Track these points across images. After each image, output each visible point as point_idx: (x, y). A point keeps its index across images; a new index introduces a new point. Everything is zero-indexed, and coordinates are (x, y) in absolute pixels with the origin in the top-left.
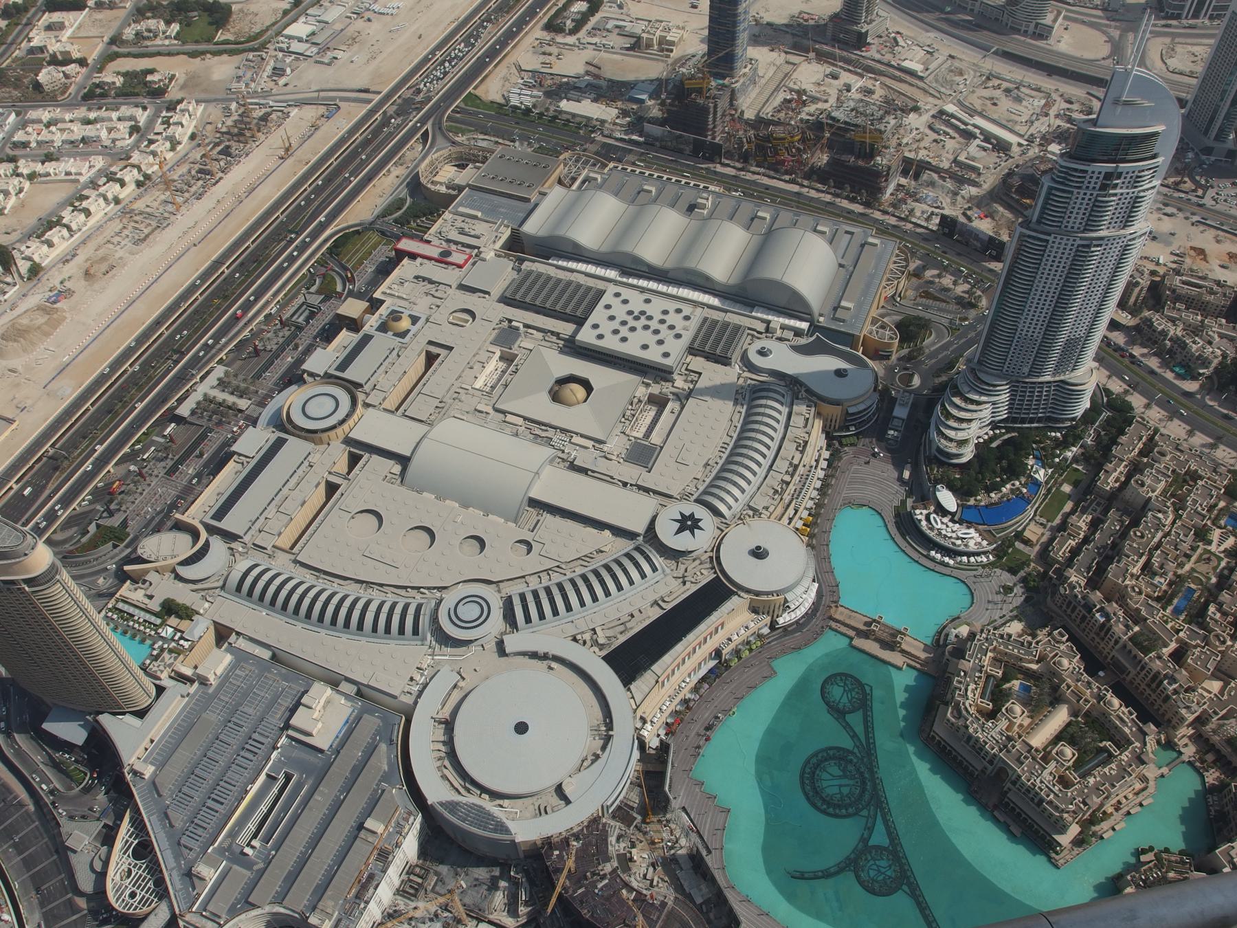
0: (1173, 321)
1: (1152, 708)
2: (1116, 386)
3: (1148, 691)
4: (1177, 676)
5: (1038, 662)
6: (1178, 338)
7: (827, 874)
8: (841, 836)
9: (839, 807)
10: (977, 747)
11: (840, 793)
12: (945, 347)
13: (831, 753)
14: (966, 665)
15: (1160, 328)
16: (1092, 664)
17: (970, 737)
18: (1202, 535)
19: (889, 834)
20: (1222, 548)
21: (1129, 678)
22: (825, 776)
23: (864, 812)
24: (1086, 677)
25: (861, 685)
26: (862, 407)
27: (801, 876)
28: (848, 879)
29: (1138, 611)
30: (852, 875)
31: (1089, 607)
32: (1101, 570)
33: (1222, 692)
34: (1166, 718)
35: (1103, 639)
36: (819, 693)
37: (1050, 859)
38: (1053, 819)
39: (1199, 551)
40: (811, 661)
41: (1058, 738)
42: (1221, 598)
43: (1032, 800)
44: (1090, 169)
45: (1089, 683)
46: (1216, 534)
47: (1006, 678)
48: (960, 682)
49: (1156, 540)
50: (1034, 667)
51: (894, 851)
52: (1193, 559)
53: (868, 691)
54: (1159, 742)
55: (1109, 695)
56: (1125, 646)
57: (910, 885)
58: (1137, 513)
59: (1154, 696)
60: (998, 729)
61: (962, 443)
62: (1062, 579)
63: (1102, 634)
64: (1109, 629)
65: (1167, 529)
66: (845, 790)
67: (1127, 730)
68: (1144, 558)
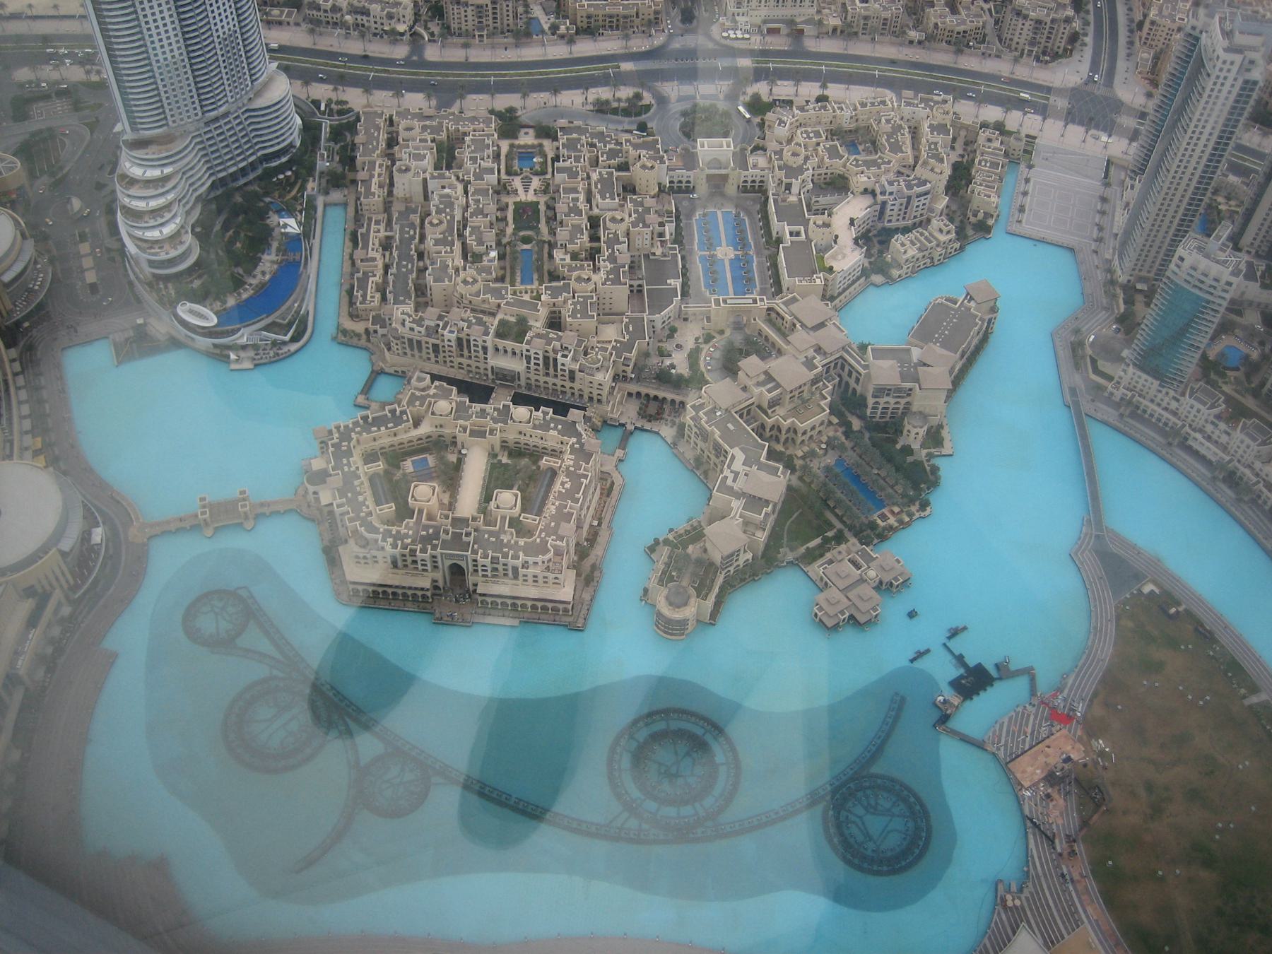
2: (322, 91)
3: (551, 380)
20: (531, 192)
21: (523, 382)
24: (477, 407)
26: (18, 268)
32: (421, 290)
34: (586, 396)
43: (505, 575)
45: (483, 411)
46: (517, 183)
49: (458, 217)
61: (175, 238)
63: (466, 352)
64: (468, 341)
68: (457, 247)
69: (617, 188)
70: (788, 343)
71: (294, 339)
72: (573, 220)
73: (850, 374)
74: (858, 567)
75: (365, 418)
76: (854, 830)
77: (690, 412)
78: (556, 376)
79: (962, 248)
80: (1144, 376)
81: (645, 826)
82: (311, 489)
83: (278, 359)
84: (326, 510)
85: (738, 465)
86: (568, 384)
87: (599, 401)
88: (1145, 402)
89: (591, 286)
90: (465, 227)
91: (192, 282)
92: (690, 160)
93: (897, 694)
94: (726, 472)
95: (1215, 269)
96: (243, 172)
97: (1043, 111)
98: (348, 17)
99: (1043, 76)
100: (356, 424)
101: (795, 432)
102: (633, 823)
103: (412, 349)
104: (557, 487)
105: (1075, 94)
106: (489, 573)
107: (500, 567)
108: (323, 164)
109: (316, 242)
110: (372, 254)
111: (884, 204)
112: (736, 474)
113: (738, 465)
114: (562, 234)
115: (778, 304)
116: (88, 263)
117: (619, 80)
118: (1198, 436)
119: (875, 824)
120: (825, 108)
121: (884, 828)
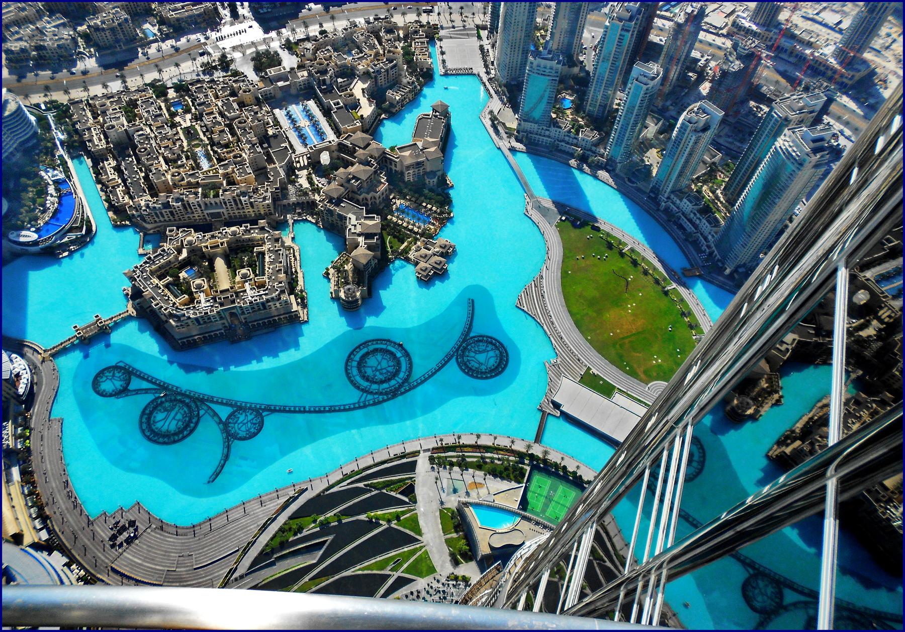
0: (20, 39)
3: (241, 211)
4: (243, 189)
5: (179, 252)
7: (226, 457)
8: (208, 434)
9: (187, 426)
11: (179, 420)
13: (147, 412)
16: (204, 227)
19: (226, 404)
21: (227, 216)
22: (159, 425)
23: (202, 412)
24: (208, 235)
25: (116, 367)
27: (217, 474)
28: (237, 445)
30: (236, 442)
35: (193, 213)
36: (98, 396)
40: (70, 391)
43: (259, 309)
46: (177, 119)
51: (239, 408)
52: (182, 137)
53: (122, 365)
57: (264, 410)
62: (138, 208)
64: (189, 204)
65: (153, 135)
66: (179, 416)
68: (161, 159)
69: (235, 106)
70: (355, 158)
72: (218, 128)
73: (391, 164)
75: (149, 258)
76: (473, 363)
81: (376, 396)
84: (148, 310)
85: (354, 221)
86: (251, 210)
87: (271, 214)
91: (11, 220)
95: (549, 64)
100: (146, 263)
101: (375, 198)
102: (370, 397)
104: (267, 259)
107: (255, 306)
109: (75, 179)
110: (111, 177)
113: (354, 221)
119: (481, 358)
121: (486, 358)
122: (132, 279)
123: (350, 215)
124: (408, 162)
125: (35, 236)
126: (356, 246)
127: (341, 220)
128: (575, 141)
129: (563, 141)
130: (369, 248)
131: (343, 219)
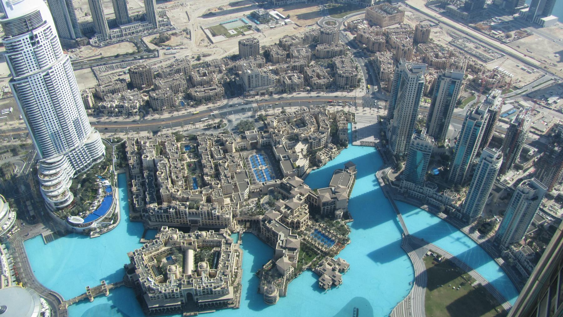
1: (216, 225)
6: (118, 105)
10: (171, 297)
12: (26, 168)
14: (140, 270)
15: (109, 106)
16: (185, 229)
17: (165, 294)
18: (182, 160)
21: (201, 223)
24: (186, 235)
29: (183, 197)
31: (166, 211)
33: (232, 200)
34: (224, 224)
35: (180, 218)
37: (233, 308)
38: (221, 293)
39: (185, 165)
41: (196, 262)
42: (205, 172)
43: (208, 294)
44: (21, 39)
47: (159, 261)
48: (143, 279)
50: (164, 248)
54: (229, 235)
55: (199, 233)
56: (190, 213)
58: (153, 168)
59: (214, 221)
60: (173, 281)
61: (64, 194)
63: (179, 216)
64: (179, 212)
67: (216, 239)
68: (169, 180)
69: (222, 152)
71: (114, 223)
73: (313, 200)
74: (331, 265)
77: (261, 223)
78: (212, 219)
79: (339, 153)
80: (409, 183)
82: (129, 276)
83: (109, 231)
84: (136, 283)
85: (283, 238)
86: (217, 221)
88: (412, 191)
89: (219, 186)
90: (171, 173)
92: (244, 138)
93: (355, 308)
94: (279, 241)
96: (86, 167)
97: (355, 105)
98: (117, 110)
99: (352, 94)
103: (159, 218)
105: (363, 98)
106: (202, 294)
107: (206, 291)
108: (115, 160)
111: (311, 143)
112: (283, 241)
113: (283, 238)
114: (206, 170)
115: (284, 181)
116: (30, 208)
117: (215, 117)
118: (431, 199)
120: (285, 115)
122: (132, 259)
123: (280, 233)
124: (324, 200)
125: (82, 221)
126: (281, 256)
127: (274, 236)
128: (440, 198)
129: (432, 197)
130: (291, 258)
131: (275, 235)
